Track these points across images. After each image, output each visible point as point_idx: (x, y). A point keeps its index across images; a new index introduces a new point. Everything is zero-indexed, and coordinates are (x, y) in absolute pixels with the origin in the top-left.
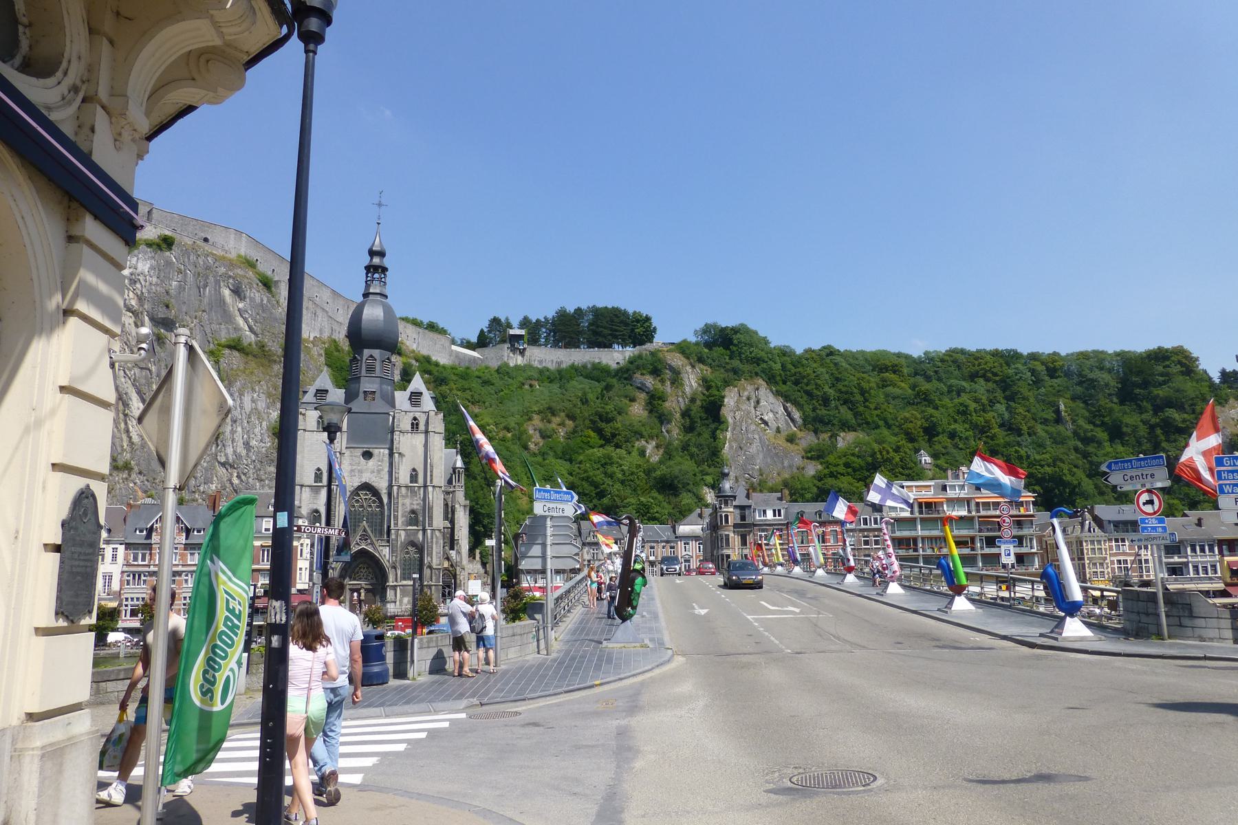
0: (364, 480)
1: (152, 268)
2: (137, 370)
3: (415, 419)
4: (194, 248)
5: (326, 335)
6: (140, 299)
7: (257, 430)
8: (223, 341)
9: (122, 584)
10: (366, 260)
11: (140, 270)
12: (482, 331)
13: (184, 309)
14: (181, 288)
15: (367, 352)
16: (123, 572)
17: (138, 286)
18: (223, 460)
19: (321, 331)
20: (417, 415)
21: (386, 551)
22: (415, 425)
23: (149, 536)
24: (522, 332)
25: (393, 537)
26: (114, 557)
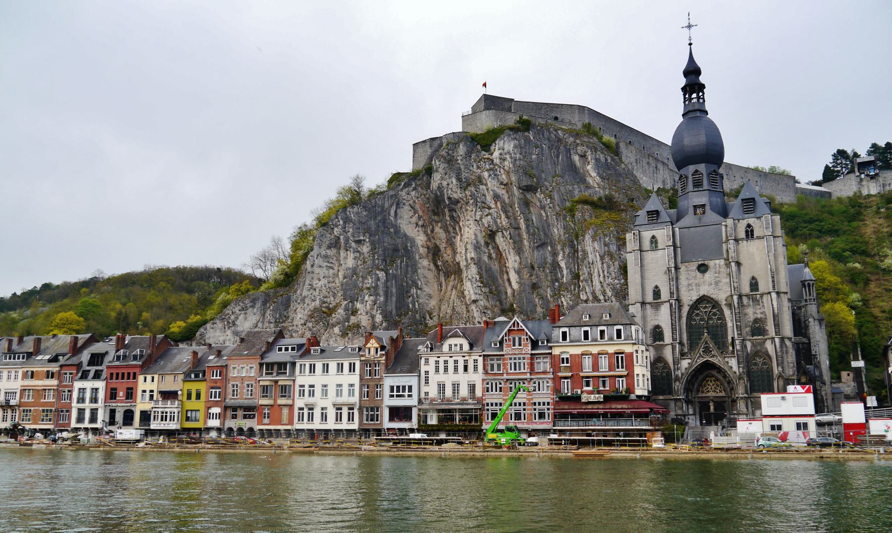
0: (702, 293)
1: (515, 147)
2: (512, 230)
3: (749, 226)
4: (546, 127)
5: (668, 186)
7: (612, 268)
8: (576, 198)
9: (483, 392)
11: (506, 150)
12: (827, 167)
13: (543, 176)
15: (692, 168)
16: (483, 380)
17: (506, 163)
18: (585, 298)
19: (664, 182)
20: (752, 221)
21: (733, 363)
23: (501, 348)
24: (872, 158)
25: (738, 347)
26: (476, 368)
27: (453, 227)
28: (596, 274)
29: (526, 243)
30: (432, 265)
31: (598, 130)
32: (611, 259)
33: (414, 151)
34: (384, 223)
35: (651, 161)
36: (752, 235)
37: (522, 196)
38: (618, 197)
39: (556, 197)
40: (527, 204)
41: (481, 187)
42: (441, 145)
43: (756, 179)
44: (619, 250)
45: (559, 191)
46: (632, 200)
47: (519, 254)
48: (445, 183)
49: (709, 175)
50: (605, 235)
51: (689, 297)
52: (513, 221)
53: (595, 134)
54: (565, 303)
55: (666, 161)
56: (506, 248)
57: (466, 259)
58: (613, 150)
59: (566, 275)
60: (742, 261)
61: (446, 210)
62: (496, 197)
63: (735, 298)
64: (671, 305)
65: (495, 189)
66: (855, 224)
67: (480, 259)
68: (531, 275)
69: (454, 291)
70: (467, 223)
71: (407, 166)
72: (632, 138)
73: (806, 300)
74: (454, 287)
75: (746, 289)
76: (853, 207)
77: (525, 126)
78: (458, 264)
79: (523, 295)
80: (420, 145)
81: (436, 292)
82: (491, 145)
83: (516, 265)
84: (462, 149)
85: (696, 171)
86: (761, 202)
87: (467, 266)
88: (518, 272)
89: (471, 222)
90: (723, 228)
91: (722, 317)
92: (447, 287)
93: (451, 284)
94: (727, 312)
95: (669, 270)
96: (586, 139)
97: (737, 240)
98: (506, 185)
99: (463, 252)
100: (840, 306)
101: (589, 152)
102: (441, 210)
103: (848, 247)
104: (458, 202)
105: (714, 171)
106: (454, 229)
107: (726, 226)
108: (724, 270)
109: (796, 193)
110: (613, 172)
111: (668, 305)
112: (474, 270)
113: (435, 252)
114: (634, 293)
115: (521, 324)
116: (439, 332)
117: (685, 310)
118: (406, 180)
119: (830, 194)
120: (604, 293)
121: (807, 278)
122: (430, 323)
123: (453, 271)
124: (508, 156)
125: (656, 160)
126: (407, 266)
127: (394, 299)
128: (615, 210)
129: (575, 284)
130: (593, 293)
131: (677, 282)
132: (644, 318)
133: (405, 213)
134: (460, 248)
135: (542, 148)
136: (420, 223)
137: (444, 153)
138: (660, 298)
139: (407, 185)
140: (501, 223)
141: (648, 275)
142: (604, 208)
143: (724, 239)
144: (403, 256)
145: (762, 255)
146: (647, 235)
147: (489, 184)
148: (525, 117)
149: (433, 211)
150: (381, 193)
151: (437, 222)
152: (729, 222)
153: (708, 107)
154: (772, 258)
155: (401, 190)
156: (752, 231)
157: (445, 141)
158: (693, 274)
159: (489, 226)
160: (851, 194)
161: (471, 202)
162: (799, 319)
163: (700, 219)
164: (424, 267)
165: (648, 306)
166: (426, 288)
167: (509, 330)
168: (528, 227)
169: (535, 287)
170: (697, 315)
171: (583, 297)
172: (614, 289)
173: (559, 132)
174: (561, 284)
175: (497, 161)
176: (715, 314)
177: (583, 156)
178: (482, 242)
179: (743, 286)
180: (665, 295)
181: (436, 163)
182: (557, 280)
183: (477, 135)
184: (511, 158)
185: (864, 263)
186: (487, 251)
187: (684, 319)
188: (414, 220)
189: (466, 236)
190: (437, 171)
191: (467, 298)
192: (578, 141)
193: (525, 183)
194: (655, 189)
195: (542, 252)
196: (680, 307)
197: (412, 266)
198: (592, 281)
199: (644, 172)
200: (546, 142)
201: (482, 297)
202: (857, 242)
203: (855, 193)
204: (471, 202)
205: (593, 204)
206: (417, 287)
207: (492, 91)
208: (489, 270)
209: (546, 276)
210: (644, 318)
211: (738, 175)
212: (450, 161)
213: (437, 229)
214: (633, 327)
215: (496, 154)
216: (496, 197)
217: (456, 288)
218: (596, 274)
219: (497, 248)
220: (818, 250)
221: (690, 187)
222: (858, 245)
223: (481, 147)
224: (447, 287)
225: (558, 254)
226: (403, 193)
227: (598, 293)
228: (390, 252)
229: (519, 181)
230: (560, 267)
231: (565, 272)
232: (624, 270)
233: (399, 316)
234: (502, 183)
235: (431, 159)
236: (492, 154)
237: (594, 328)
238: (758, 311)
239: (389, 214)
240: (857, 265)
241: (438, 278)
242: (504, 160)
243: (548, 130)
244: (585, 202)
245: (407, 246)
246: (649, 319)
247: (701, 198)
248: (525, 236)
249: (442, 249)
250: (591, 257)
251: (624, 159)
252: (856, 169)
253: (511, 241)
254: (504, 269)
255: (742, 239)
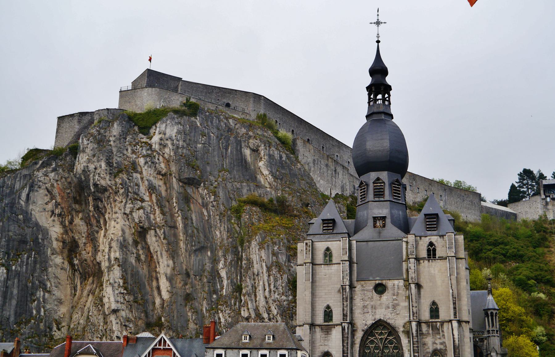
0: (378, 317)
1: (179, 132)
2: (167, 229)
3: (431, 244)
4: (215, 114)
5: (348, 193)
6: (167, 162)
7: (279, 282)
8: (244, 198)
10: (368, 80)
11: (168, 135)
12: (513, 186)
13: (208, 169)
14: (206, 152)
15: (373, 175)
17: (167, 150)
19: (343, 188)
20: (434, 239)
22: (432, 253)
27: (97, 221)
28: (261, 288)
29: (182, 244)
30: (66, 263)
31: (274, 123)
32: (279, 271)
33: (59, 125)
34: (12, 207)
35: (330, 163)
36: (435, 255)
37: (181, 190)
38: (292, 200)
39: (221, 194)
40: (186, 199)
41: (135, 175)
42: (91, 122)
43: (441, 193)
44: (289, 261)
45: (225, 188)
46: (307, 205)
47: (173, 258)
48: (92, 167)
49: (391, 184)
50: (274, 243)
51: (364, 321)
52: (169, 218)
53: (270, 127)
54: (222, 320)
55: (346, 165)
56: (158, 249)
57: (109, 259)
58: (290, 148)
59: (226, 288)
60: (423, 283)
61: (90, 199)
62: (152, 189)
63: (414, 324)
64: (343, 329)
65: (151, 178)
66: (540, 250)
67: (125, 261)
68: (186, 284)
69: (91, 297)
70: (114, 216)
71: (48, 142)
72: (312, 137)
73: (489, 331)
74: (92, 292)
75: (426, 315)
76: (538, 232)
77: (192, 109)
78: (99, 264)
79: (174, 307)
80: (66, 120)
81: (69, 297)
82: (150, 128)
83: (169, 271)
84: (116, 129)
85: (378, 179)
86: (444, 219)
87: (110, 268)
88: (170, 279)
89: (119, 215)
90: (404, 244)
91: (399, 346)
92: (82, 291)
93: (88, 288)
94: (404, 341)
95: (343, 288)
96: (260, 132)
97: (418, 259)
98: (165, 176)
99: (107, 250)
100: (524, 340)
101: (263, 147)
102: (84, 198)
103: (532, 275)
104: (105, 190)
105: (397, 181)
106: (98, 222)
107: (407, 242)
108: (403, 292)
109: (481, 212)
110: (287, 172)
111: (339, 329)
112: (117, 272)
113: (71, 248)
114: (302, 313)
115: (168, 342)
116: (67, 348)
117: (359, 335)
118: (45, 159)
119: (515, 215)
120: (269, 311)
121: (491, 307)
122: (57, 335)
123: (92, 273)
124: (169, 143)
125: (336, 162)
126: (35, 262)
127: (14, 302)
128: (287, 214)
129: (236, 298)
130: (256, 310)
131: (351, 303)
132: (312, 343)
133: (40, 197)
134: (103, 246)
135: (210, 136)
136: (57, 211)
137: (94, 131)
138: (331, 320)
139: (43, 166)
140: (155, 219)
141: (321, 292)
142: (275, 212)
143: (404, 257)
144: (31, 250)
145: (444, 279)
146: (321, 246)
147: (144, 173)
148: (193, 100)
149: (75, 198)
150: (13, 171)
151: (78, 212)
152: (411, 238)
153: (393, 110)
154: (454, 282)
155: (38, 170)
156: (434, 250)
157: (96, 117)
158: (369, 294)
159: (140, 222)
160: (536, 217)
161: (121, 191)
162: (481, 353)
163: (380, 233)
164: (56, 266)
165: (318, 329)
166: (57, 293)
167: (154, 350)
168: (185, 226)
169: (188, 298)
170: (372, 342)
171: (245, 314)
172: (280, 306)
173: (231, 121)
174: (220, 297)
175: (156, 147)
176: (391, 342)
177: (255, 151)
178: (130, 241)
179: (422, 311)
180: (337, 317)
181: (83, 142)
182: (215, 292)
183: (136, 114)
184: (173, 144)
185: (549, 294)
186: (135, 251)
187: (357, 346)
188: (50, 207)
189: (111, 231)
190: (84, 151)
191: (106, 306)
192: (251, 133)
193: (186, 175)
194: (333, 195)
195: (200, 257)
196: (354, 332)
197: (41, 263)
198: (255, 295)
199: (322, 175)
200: (215, 130)
201: (124, 307)
202: (542, 270)
203: (541, 217)
204: (121, 191)
205: (263, 206)
206: (45, 290)
207: (156, 67)
208: (135, 274)
209: (203, 286)
210: (312, 343)
211: (421, 187)
212: (101, 142)
213: (78, 221)
214: (299, 352)
215: (156, 139)
216: (152, 189)
217: (93, 294)
218: (261, 288)
219: (147, 248)
220: (502, 275)
221: (371, 196)
222: (543, 273)
223: (140, 128)
224: (82, 291)
225: (219, 261)
226: (40, 174)
227: (262, 310)
228: (16, 243)
229: (180, 171)
230: (220, 277)
231: (225, 282)
232: (293, 285)
233: (19, 324)
234: (159, 173)
235: (78, 136)
236: (151, 138)
237: (255, 352)
238: (438, 341)
239: (19, 198)
240: (542, 295)
241: (73, 280)
242: (165, 146)
243: (218, 117)
244: (254, 203)
245: (37, 238)
246: (318, 344)
247: (381, 210)
248: (182, 236)
249: (81, 245)
250: (256, 267)
251: (300, 158)
252: (542, 192)
253: (165, 241)
254: (154, 274)
255: (424, 259)
